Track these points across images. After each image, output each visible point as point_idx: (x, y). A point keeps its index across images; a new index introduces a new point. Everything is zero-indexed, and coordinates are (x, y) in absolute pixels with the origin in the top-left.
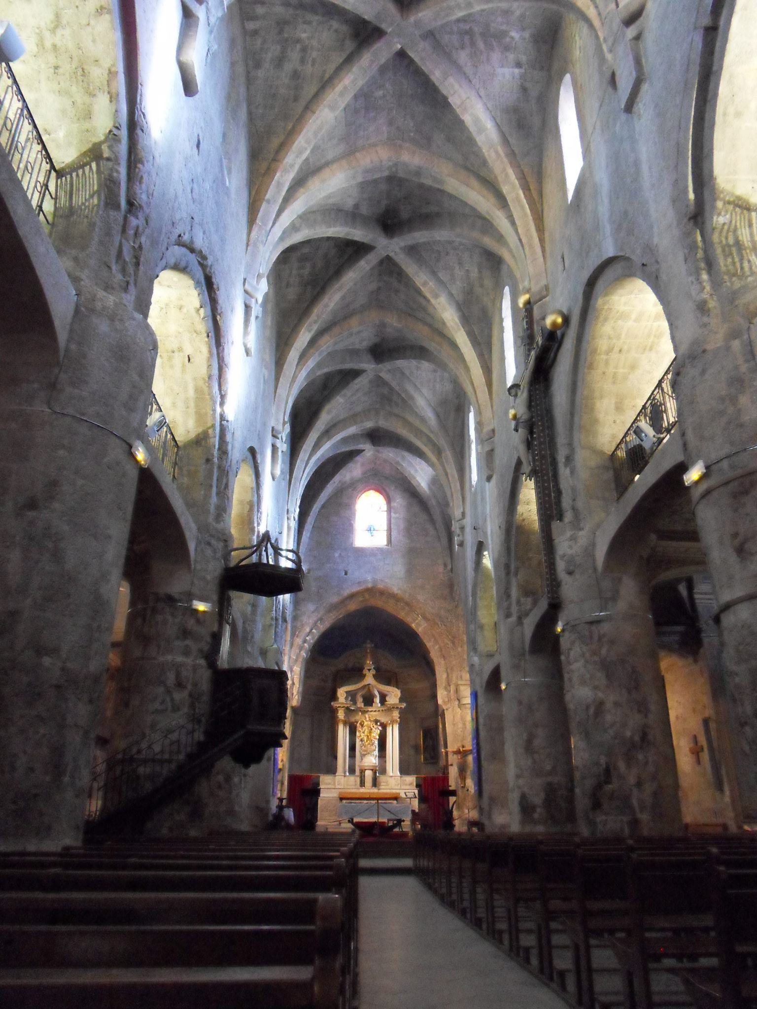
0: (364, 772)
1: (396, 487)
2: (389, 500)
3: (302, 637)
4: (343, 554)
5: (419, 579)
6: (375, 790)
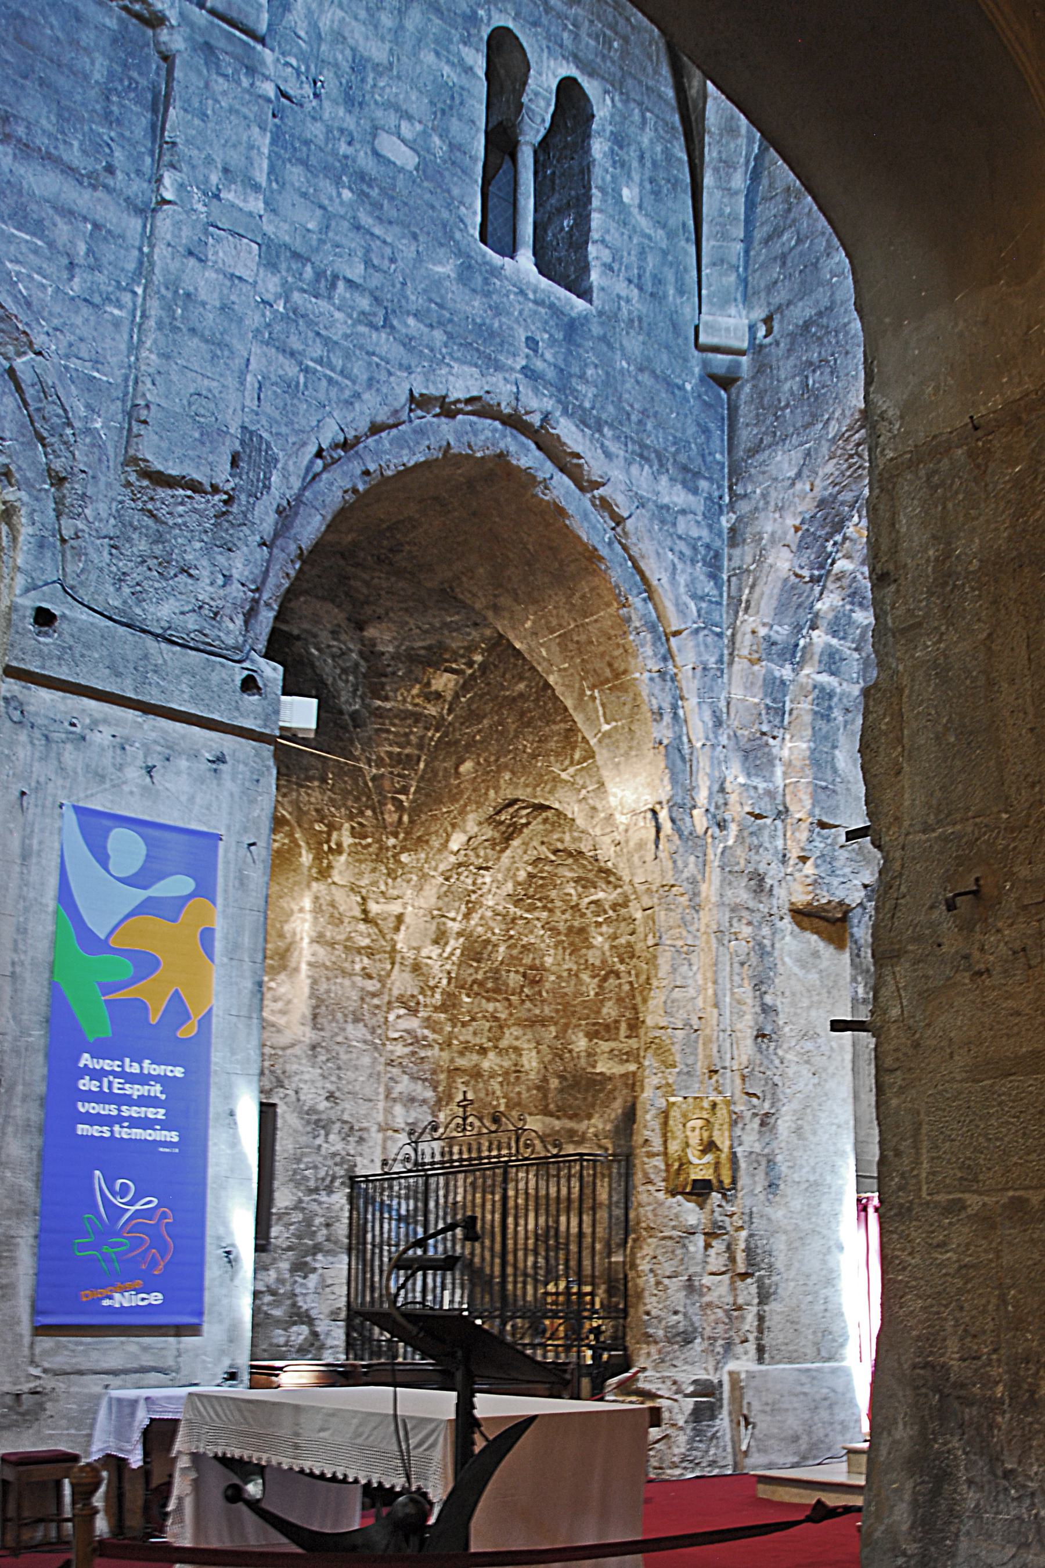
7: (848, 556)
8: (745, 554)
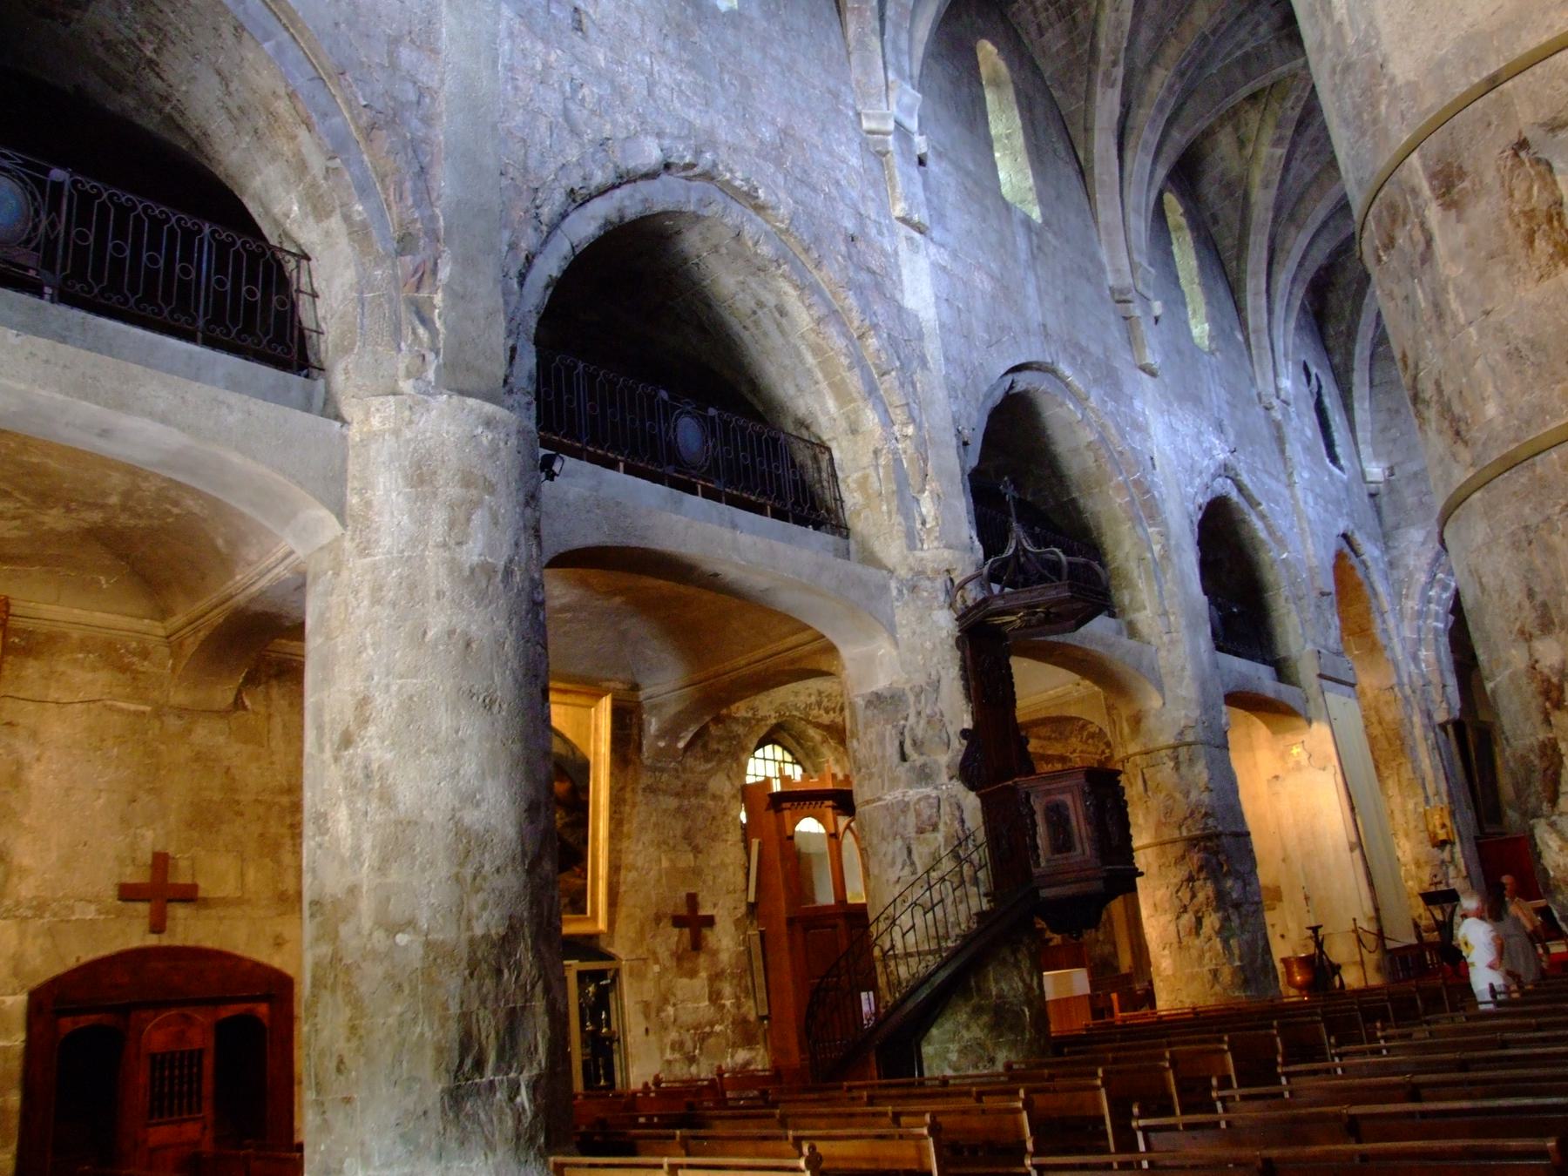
3: (1417, 596)
8: (1401, 573)
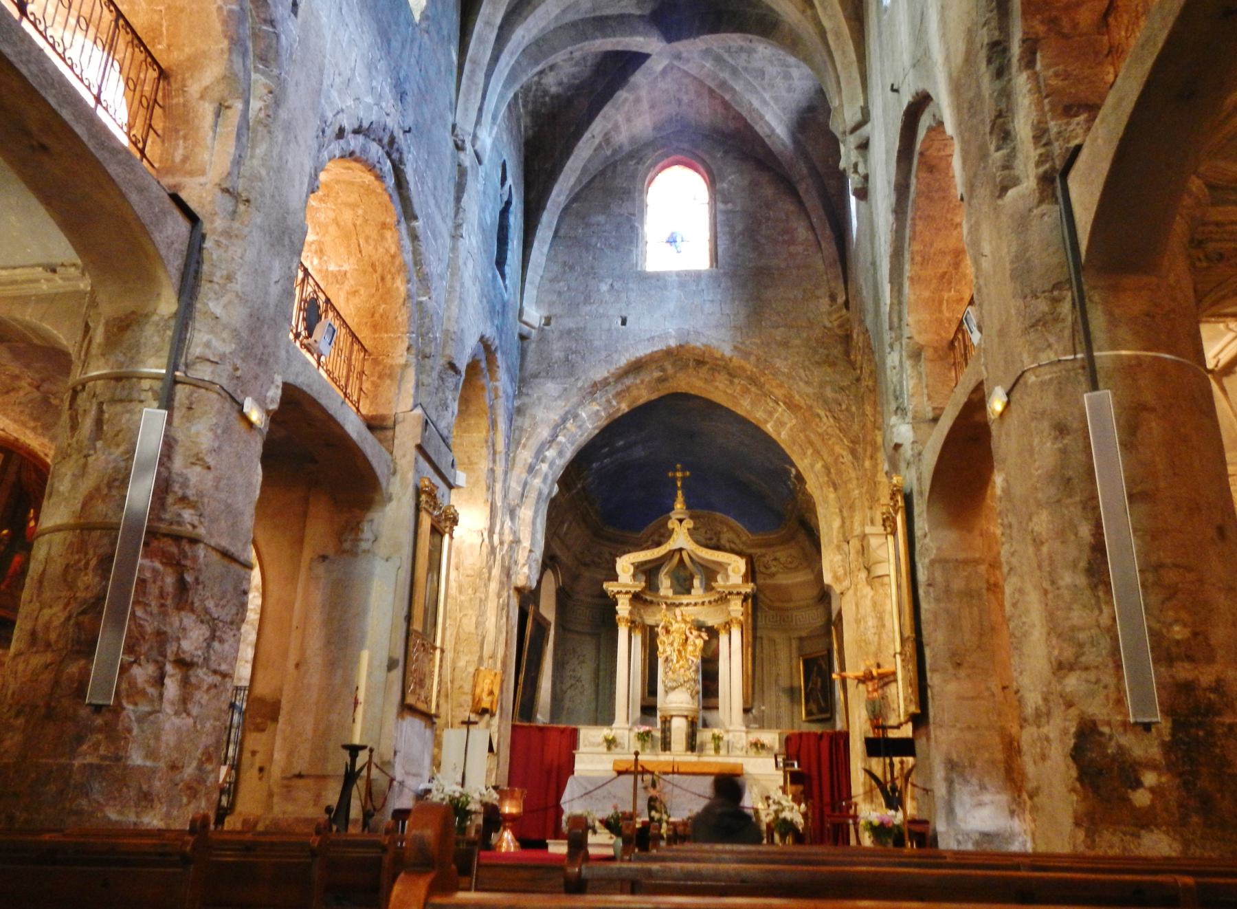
0: (670, 722)
1: (726, 153)
2: (712, 180)
4: (617, 286)
5: (778, 327)
6: (692, 758)
7: (565, 436)
